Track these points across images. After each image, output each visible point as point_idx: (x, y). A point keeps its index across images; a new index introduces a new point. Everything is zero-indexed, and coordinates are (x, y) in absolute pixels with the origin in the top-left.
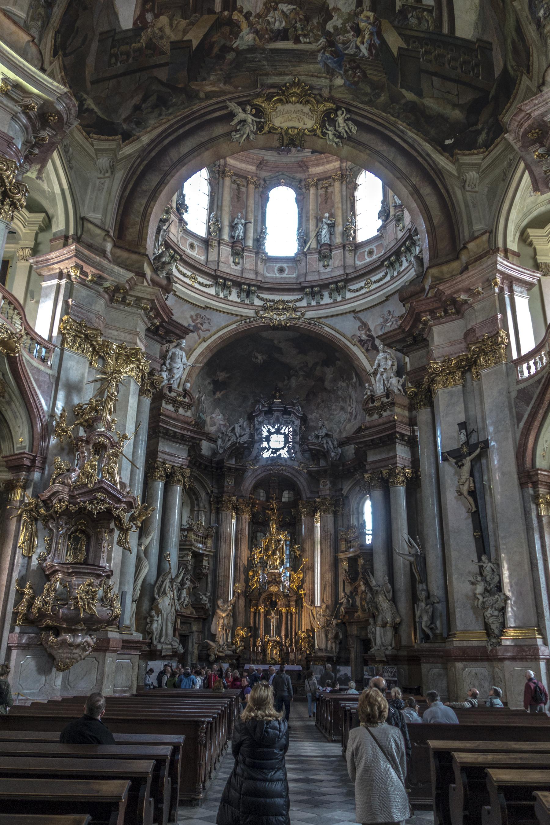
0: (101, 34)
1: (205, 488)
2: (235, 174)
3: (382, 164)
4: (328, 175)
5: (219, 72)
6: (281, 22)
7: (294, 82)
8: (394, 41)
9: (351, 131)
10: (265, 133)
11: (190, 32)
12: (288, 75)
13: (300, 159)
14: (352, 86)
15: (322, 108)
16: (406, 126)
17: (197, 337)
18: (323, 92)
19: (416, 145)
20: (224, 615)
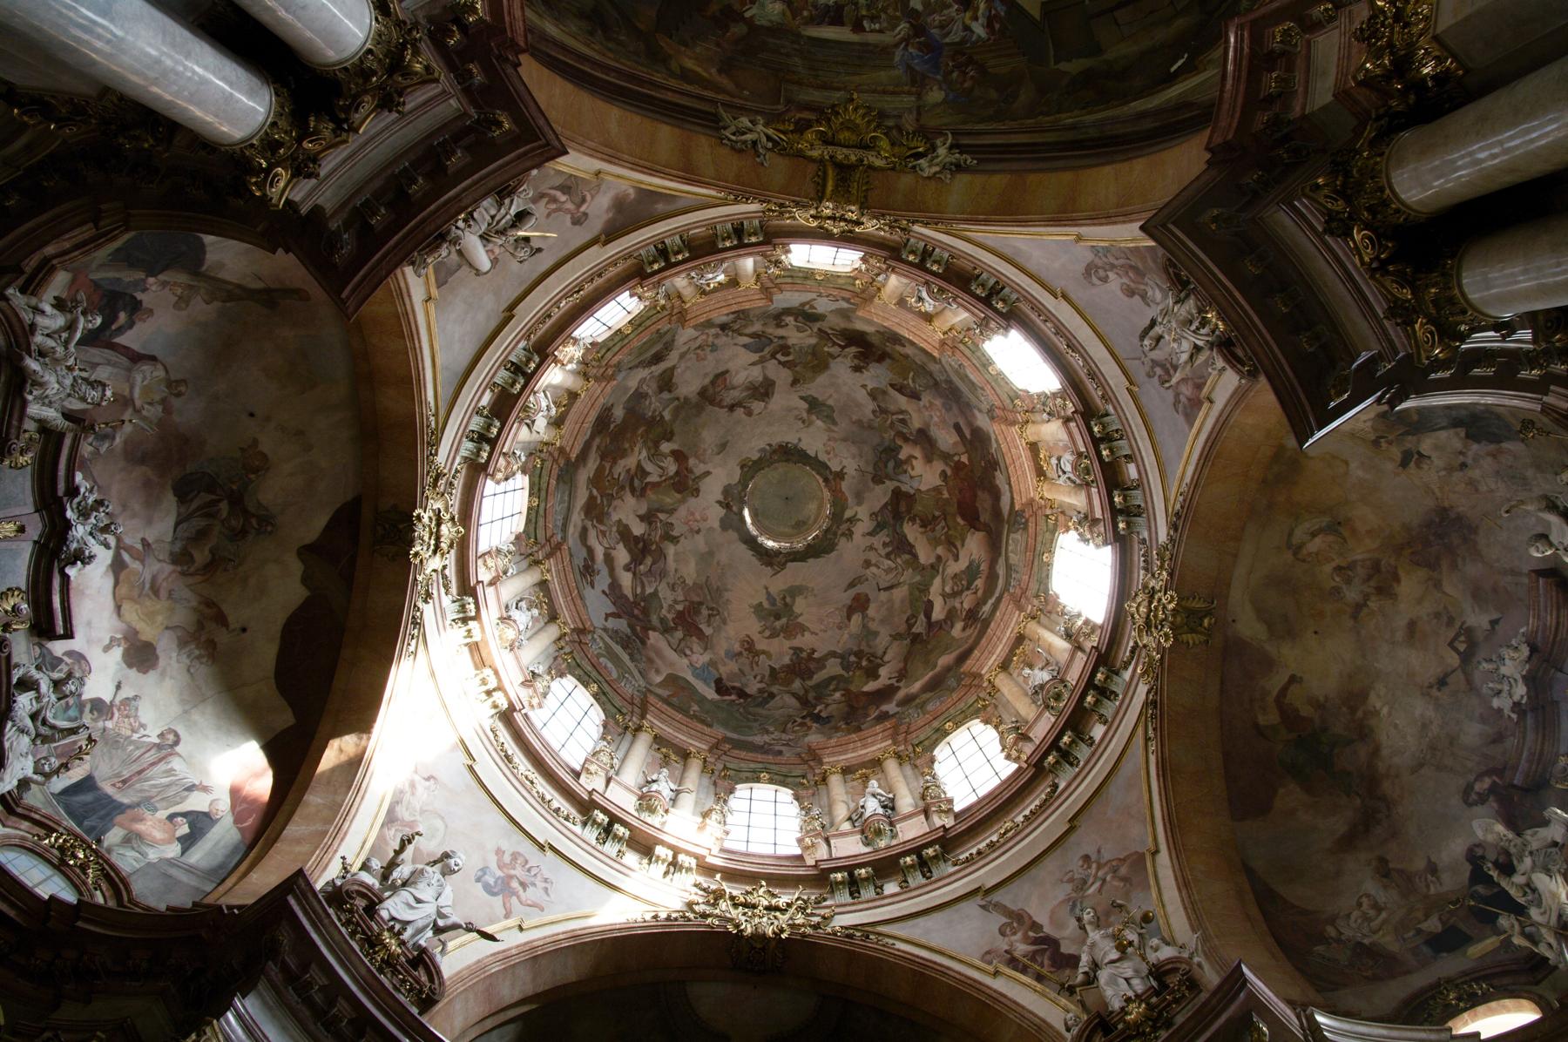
12: (839, 89)
17: (501, 912)
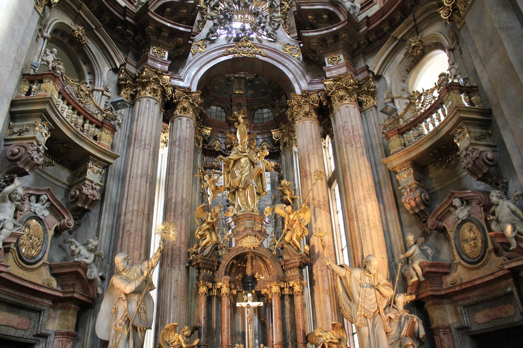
1: (110, 59)
20: (129, 288)
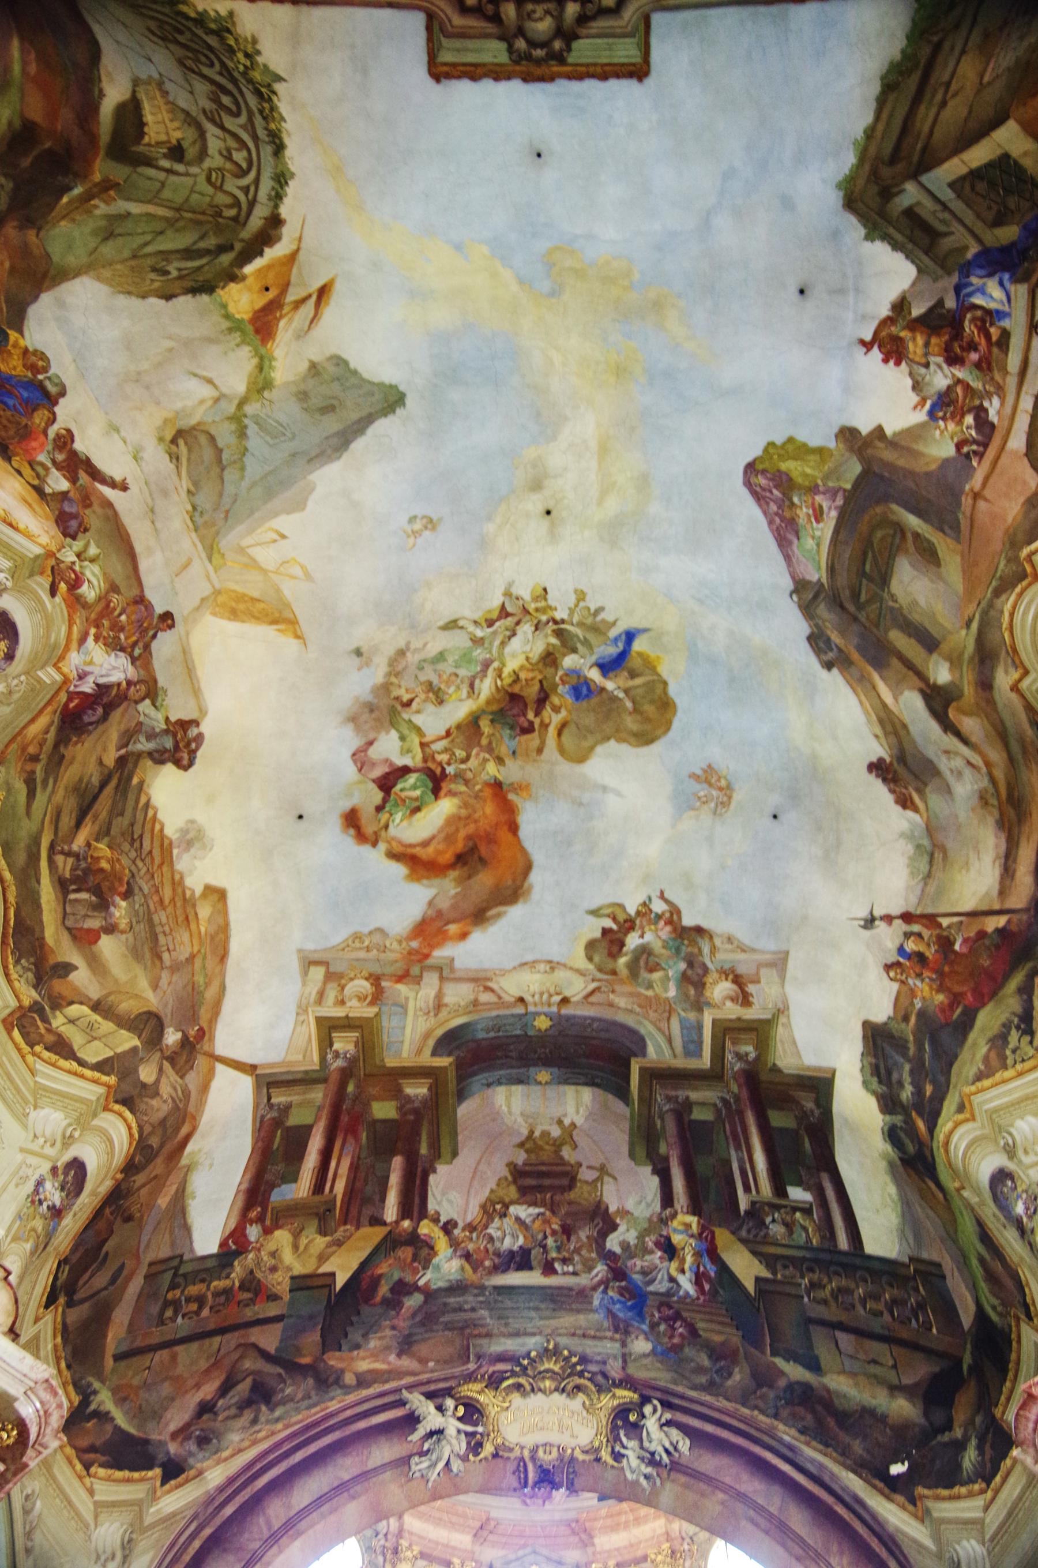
0: (150, 1264)
2: (423, 1555)
3: (757, 1525)
4: (640, 1553)
5: (388, 1332)
6: (515, 1237)
7: (546, 1350)
8: (746, 1268)
9: (676, 1449)
10: (486, 1458)
11: (332, 1259)
12: (533, 1334)
13: (572, 1515)
14: (669, 1354)
15: (607, 1402)
16: (797, 1434)
18: (608, 1367)
19: (827, 1479)
